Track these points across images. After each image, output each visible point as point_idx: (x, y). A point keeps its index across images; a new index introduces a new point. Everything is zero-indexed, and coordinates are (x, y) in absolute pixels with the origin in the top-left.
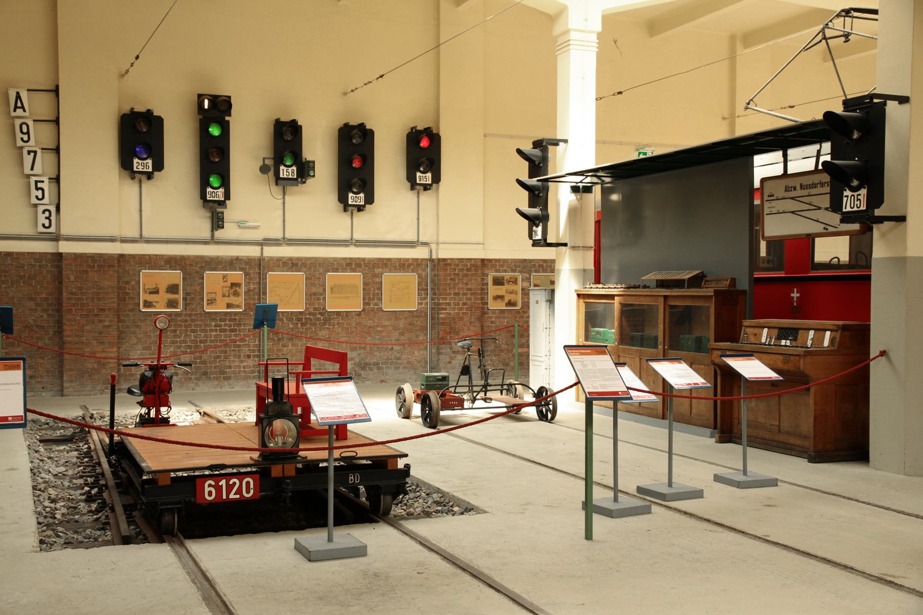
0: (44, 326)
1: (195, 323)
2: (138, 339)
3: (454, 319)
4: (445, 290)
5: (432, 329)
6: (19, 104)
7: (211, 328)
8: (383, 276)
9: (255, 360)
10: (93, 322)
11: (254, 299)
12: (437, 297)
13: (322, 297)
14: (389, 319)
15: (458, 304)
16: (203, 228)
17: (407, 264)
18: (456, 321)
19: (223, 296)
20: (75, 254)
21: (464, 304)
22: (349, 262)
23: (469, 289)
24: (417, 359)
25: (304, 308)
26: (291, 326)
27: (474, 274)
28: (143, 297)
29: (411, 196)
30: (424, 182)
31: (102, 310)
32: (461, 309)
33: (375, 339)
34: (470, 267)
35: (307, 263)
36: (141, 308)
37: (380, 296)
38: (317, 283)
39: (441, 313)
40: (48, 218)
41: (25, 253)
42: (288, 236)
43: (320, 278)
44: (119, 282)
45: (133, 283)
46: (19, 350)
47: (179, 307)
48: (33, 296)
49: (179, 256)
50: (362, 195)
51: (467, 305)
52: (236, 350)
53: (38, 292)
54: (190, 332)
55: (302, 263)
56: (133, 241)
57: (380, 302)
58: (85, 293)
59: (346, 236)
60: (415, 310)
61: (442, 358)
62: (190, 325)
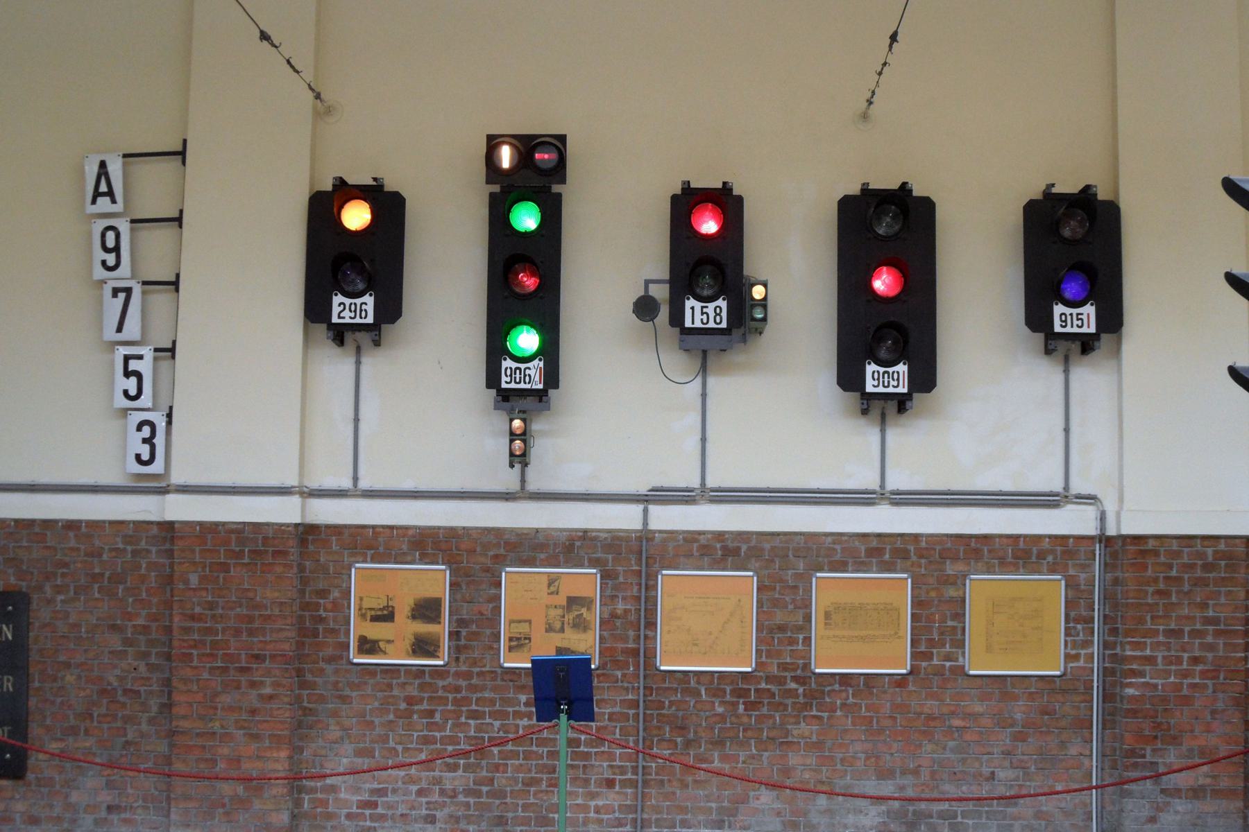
0: (139, 691)
1: (479, 695)
2: (345, 730)
3: (1165, 700)
4: (1141, 621)
5: (1104, 725)
6: (103, 188)
7: (517, 708)
8: (968, 581)
9: (626, 794)
10: (238, 688)
11: (625, 640)
12: (1120, 639)
13: (801, 637)
14: (983, 698)
15: (1179, 660)
17: (1035, 550)
18: (1171, 706)
19: (547, 631)
20: (201, 524)
21: (1195, 660)
22: (874, 544)
23: (1208, 621)
24: (1063, 805)
25: (754, 665)
26: (720, 710)
27: (1223, 579)
28: (357, 628)
29: (1047, 375)
30: (1076, 330)
31: (257, 658)
32: (1185, 674)
33: (944, 748)
34: (1215, 559)
35: (762, 550)
36: (351, 657)
37: (959, 637)
38: (787, 599)
39: (1130, 685)
40: (148, 441)
41: (104, 522)
42: (711, 482)
43: (796, 587)
44: (302, 592)
45: (336, 594)
46: (87, 744)
47: (440, 655)
48: (119, 622)
49: (445, 528)
50: (902, 368)
51: (1205, 664)
52: (578, 767)
53: (129, 613)
54: (467, 718)
55: (749, 549)
56: (684, 497)
57: (960, 651)
58: (221, 616)
59: (866, 479)
60: (1058, 673)
61: (1130, 807)
62: (467, 701)
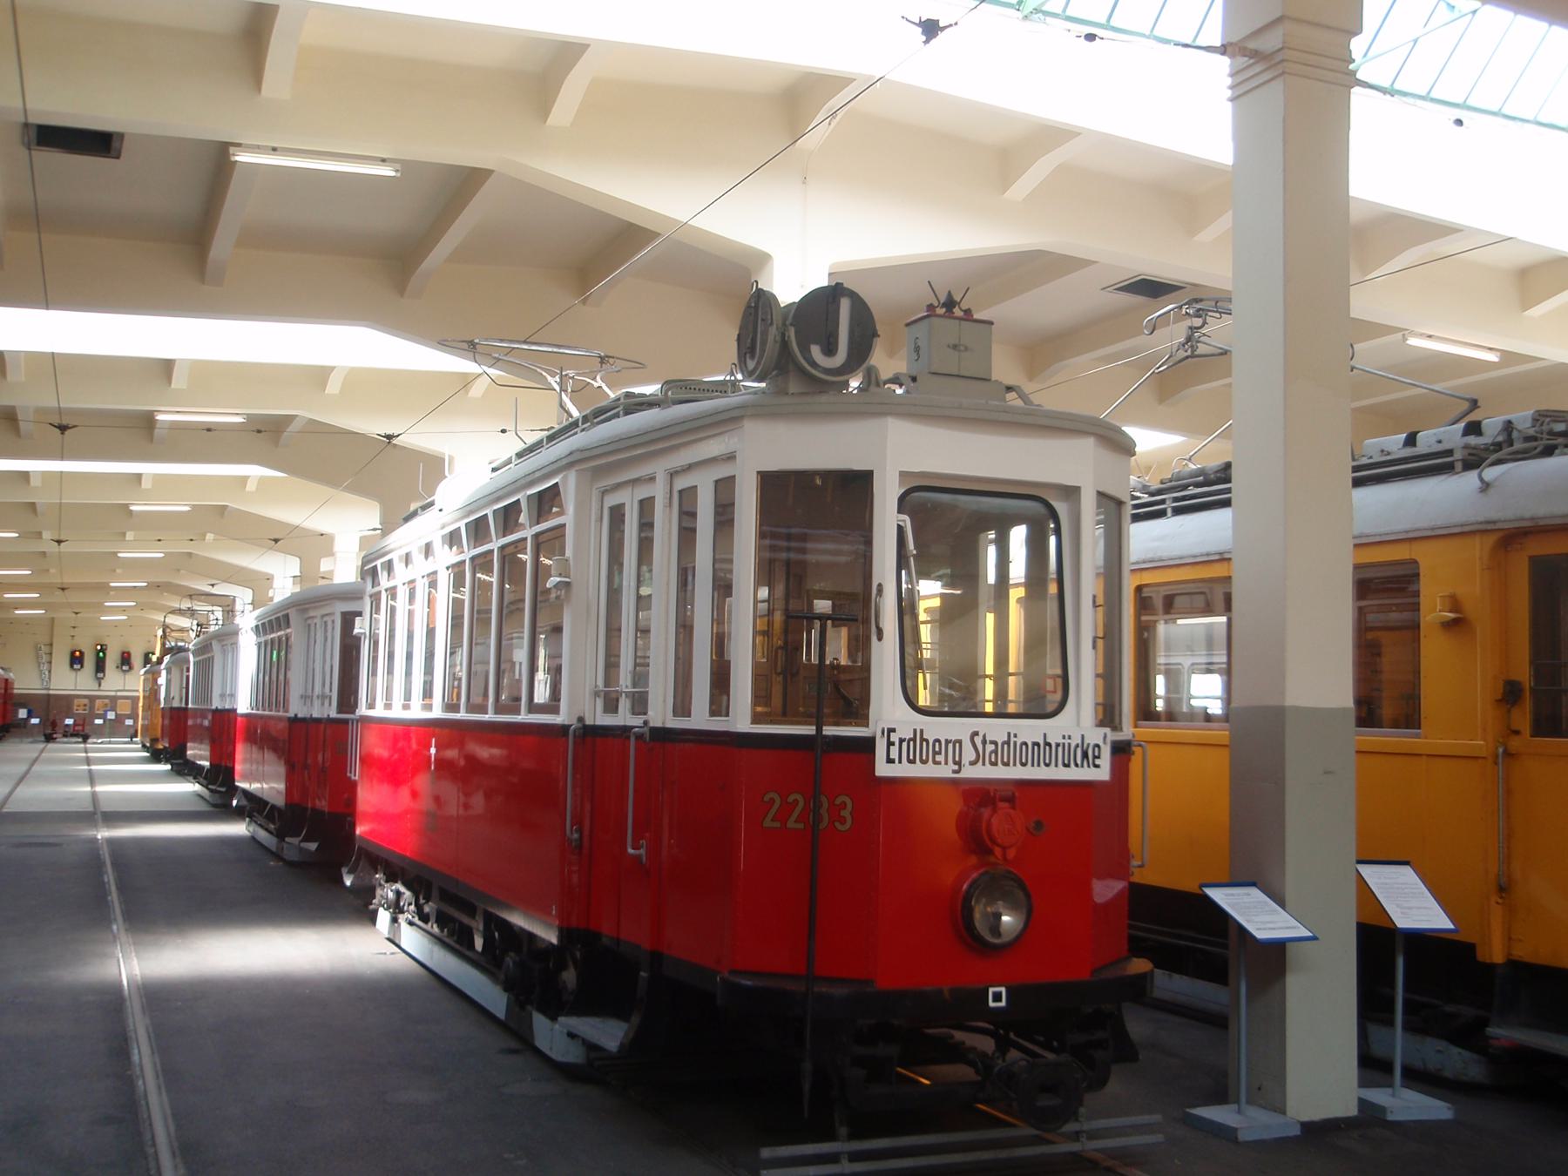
16: (97, 688)
28: (75, 708)
